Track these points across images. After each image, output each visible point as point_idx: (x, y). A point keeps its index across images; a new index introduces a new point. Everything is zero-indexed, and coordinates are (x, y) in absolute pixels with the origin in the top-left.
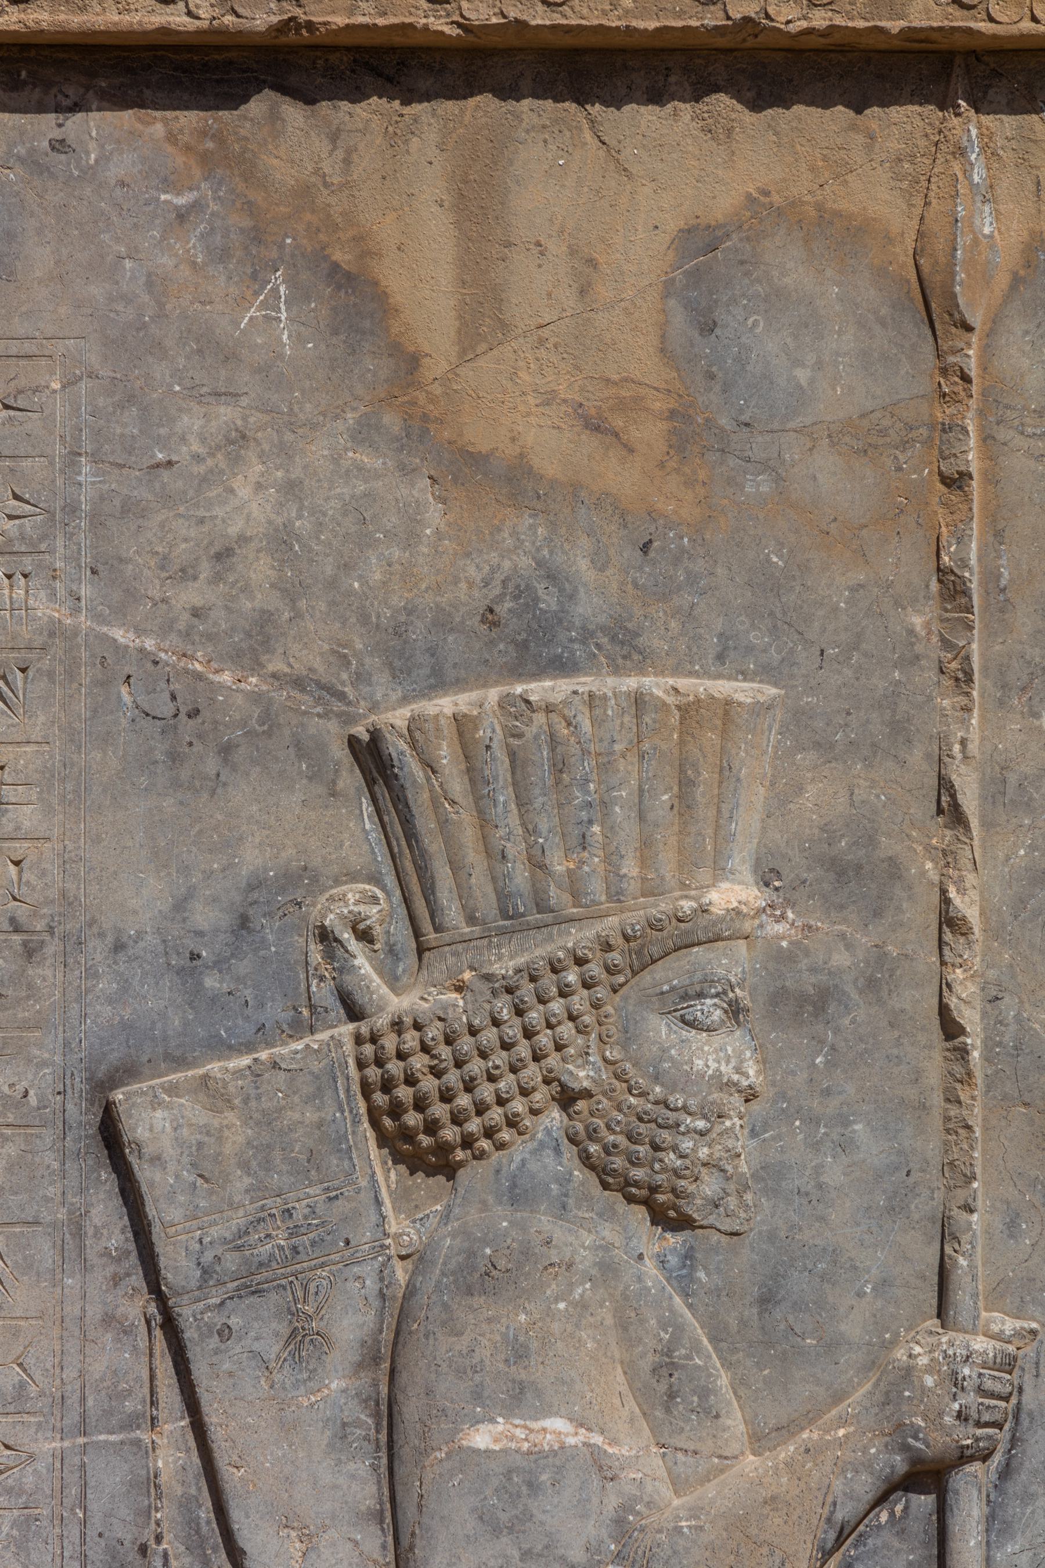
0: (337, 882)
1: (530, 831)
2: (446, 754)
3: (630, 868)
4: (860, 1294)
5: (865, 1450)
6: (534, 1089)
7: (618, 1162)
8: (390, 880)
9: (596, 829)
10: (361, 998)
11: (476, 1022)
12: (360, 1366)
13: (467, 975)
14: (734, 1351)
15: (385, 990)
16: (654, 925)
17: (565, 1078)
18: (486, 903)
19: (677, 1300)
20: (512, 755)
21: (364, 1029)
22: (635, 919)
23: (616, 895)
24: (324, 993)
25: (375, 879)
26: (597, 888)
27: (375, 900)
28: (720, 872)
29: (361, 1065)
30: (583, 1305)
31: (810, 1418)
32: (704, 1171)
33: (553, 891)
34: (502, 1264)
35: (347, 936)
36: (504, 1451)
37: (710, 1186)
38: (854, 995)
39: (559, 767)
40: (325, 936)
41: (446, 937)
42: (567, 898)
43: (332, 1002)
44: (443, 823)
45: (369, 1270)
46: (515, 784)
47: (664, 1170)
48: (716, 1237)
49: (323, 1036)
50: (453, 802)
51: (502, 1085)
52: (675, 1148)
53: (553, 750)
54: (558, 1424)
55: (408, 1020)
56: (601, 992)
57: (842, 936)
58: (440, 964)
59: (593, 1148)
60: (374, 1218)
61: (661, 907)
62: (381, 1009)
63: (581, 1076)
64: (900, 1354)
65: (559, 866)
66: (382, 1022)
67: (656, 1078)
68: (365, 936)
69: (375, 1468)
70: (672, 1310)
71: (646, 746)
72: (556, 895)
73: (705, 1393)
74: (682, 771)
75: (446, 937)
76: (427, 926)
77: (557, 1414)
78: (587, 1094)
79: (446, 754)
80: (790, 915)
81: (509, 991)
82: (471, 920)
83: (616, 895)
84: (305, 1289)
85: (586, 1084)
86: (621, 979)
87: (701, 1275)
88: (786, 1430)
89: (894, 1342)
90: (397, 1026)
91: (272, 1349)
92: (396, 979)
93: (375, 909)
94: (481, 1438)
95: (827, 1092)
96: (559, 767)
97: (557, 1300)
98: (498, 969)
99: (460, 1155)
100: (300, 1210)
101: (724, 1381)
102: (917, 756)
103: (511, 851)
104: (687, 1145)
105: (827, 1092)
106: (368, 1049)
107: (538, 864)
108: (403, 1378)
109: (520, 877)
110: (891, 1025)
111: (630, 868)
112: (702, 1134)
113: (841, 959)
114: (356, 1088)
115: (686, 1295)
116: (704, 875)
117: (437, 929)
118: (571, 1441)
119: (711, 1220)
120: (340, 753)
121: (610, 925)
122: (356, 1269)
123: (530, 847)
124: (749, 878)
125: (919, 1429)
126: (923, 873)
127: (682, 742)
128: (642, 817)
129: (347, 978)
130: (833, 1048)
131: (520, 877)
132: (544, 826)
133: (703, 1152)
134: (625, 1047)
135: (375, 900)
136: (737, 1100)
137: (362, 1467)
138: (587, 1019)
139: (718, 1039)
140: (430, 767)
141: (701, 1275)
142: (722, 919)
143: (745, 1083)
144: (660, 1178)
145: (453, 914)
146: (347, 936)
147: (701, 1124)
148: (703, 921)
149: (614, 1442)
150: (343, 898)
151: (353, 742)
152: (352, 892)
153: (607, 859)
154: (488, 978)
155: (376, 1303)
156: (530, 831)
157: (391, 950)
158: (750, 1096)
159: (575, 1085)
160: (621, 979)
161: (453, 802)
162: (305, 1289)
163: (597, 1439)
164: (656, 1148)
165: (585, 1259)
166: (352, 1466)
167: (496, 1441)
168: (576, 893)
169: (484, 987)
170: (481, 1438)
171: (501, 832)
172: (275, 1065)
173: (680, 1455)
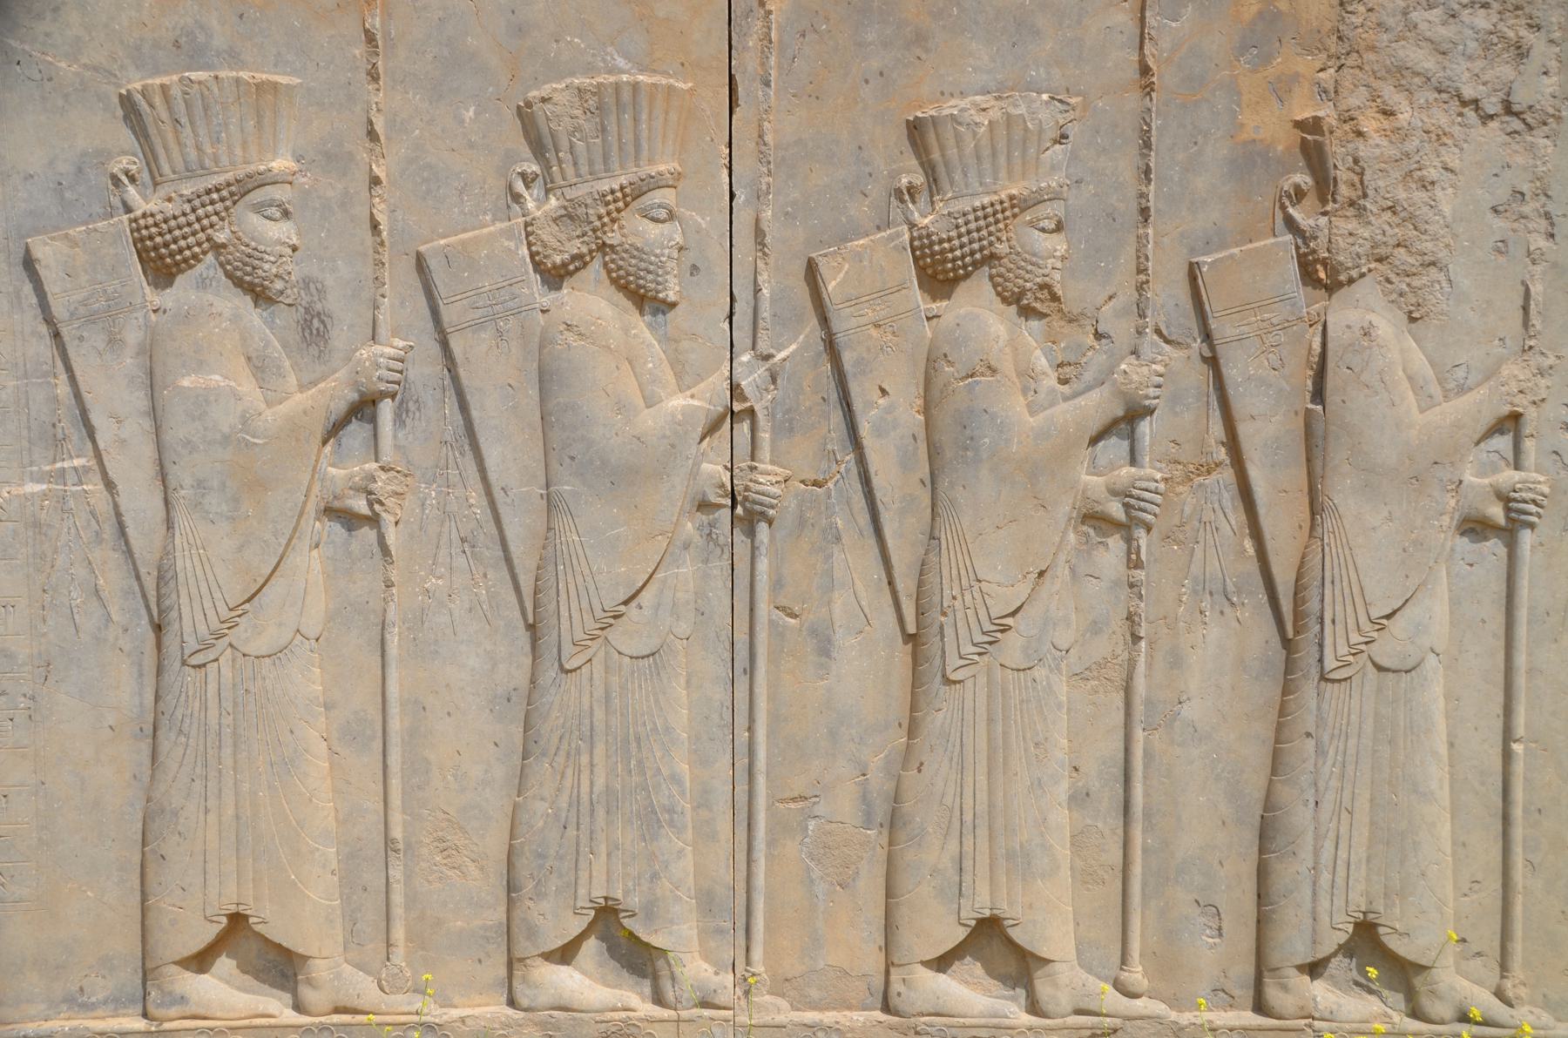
0: (119, 155)
1: (196, 135)
2: (158, 100)
3: (238, 151)
4: (342, 330)
5: (343, 391)
6: (203, 243)
7: (239, 273)
8: (141, 155)
9: (223, 135)
10: (130, 203)
11: (176, 214)
12: (138, 354)
13: (173, 195)
14: (292, 352)
15: (141, 201)
16: (250, 176)
17: (215, 238)
18: (180, 166)
19: (267, 331)
20: (185, 102)
21: (132, 216)
22: (241, 173)
23: (233, 163)
24: (116, 201)
25: (135, 155)
26: (224, 160)
27: (135, 163)
28: (275, 156)
29: (132, 232)
30: (226, 330)
31: (323, 378)
32: (276, 280)
33: (207, 161)
34: (191, 313)
35: (124, 178)
36: (196, 388)
37: (279, 285)
38: (336, 209)
39: (206, 108)
40: (116, 180)
41: (164, 179)
42: (213, 164)
43: (120, 205)
44: (159, 131)
45: (140, 314)
46: (188, 115)
47: (258, 277)
48: (283, 306)
49: (116, 219)
50: (163, 122)
51: (189, 240)
52: (261, 268)
53: (203, 100)
54: (217, 377)
55: (148, 212)
56: (228, 203)
57: (331, 184)
58: (163, 191)
59: (229, 267)
60: (141, 294)
61: (251, 168)
62: (139, 208)
63: (221, 237)
64: (358, 354)
65: (209, 151)
66: (139, 213)
67: (253, 239)
68: (132, 179)
69: (146, 395)
70: (264, 333)
71: (242, 100)
72: (207, 163)
73: (279, 367)
74: (258, 112)
75: (164, 179)
76: (157, 175)
77: (217, 374)
78: (224, 246)
79: (158, 100)
80: (309, 175)
81: (189, 201)
82: (174, 172)
83: (233, 163)
84: (114, 322)
85: (224, 241)
86: (236, 198)
87: (278, 321)
88: (314, 383)
89: (357, 350)
90: (144, 216)
91: (101, 346)
92: (146, 196)
93: (135, 167)
94: (186, 382)
95: (326, 248)
96: (206, 108)
97: (214, 328)
98: (185, 192)
99: (174, 270)
100: (110, 290)
101: (287, 364)
102: (358, 109)
103: (188, 143)
104: (266, 266)
105: (326, 248)
106: (134, 225)
107: (199, 148)
108: (154, 358)
109: (193, 155)
110: (352, 221)
111: (238, 151)
112: (274, 263)
113: (330, 193)
114: (131, 240)
115: (271, 329)
116: (269, 156)
117: (161, 176)
118: (222, 384)
119: (280, 299)
120: (116, 100)
121: (229, 176)
122: (135, 315)
123: (196, 142)
124: (290, 158)
125: (363, 383)
126: (363, 158)
127: (257, 100)
128: (242, 130)
129: (126, 197)
130: (328, 230)
131: (193, 155)
132: (201, 133)
133: (274, 270)
134: (239, 225)
135: (135, 163)
136: (289, 251)
137: (141, 394)
138: (223, 214)
139: (279, 225)
140: (151, 106)
141: (278, 321)
142: (278, 174)
143: (291, 243)
144: (257, 281)
145: (166, 169)
146: (124, 178)
147: (272, 259)
148: (269, 174)
149: (239, 385)
150: (120, 162)
151: (121, 95)
152: (125, 160)
153: (229, 147)
154: (181, 196)
155: (144, 328)
156: (196, 135)
157: (143, 184)
158: (295, 249)
159: (219, 241)
160: (236, 198)
161: (163, 122)
162: (114, 322)
163: (233, 384)
164: (254, 268)
165: (227, 313)
166: (137, 394)
167: (192, 383)
168: (216, 161)
169: (177, 199)
170: (186, 382)
171: (185, 135)
172: (95, 230)
173: (269, 392)
